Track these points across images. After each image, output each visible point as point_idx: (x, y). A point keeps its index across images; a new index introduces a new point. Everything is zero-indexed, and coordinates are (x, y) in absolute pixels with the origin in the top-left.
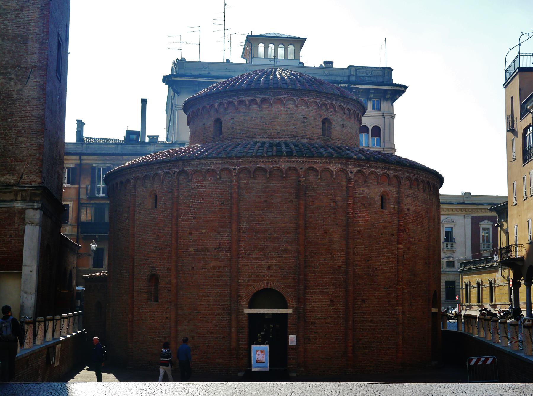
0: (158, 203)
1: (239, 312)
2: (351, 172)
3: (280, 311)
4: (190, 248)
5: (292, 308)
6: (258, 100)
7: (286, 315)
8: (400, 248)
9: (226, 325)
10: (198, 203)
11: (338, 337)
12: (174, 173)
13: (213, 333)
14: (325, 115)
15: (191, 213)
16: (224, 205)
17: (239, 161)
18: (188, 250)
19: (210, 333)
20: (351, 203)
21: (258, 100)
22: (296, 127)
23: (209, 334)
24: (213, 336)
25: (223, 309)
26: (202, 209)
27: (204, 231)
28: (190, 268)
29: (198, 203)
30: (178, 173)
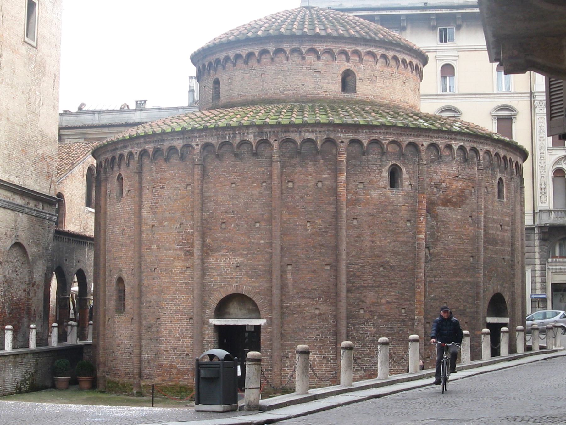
0: (124, 191)
1: (204, 322)
2: (342, 142)
3: (252, 321)
4: (153, 244)
5: (266, 318)
6: (257, 53)
7: (258, 328)
8: (420, 238)
9: (190, 340)
10: (161, 188)
11: (326, 355)
12: (136, 153)
13: (176, 349)
14: (347, 66)
15: (153, 201)
16: (186, 190)
17: (202, 134)
18: (151, 247)
19: (173, 349)
20: (341, 182)
21: (257, 53)
22: (303, 85)
23: (171, 351)
24: (176, 353)
25: (187, 319)
26: (164, 196)
27: (166, 224)
28: (154, 269)
29: (161, 188)
30: (140, 153)
